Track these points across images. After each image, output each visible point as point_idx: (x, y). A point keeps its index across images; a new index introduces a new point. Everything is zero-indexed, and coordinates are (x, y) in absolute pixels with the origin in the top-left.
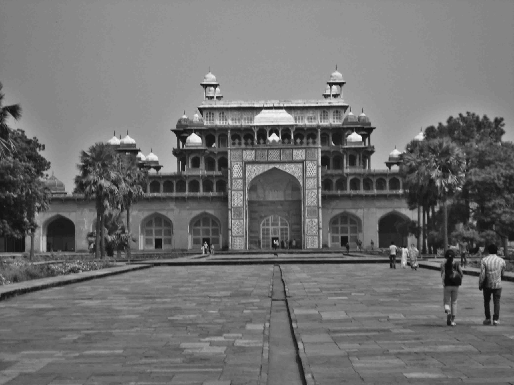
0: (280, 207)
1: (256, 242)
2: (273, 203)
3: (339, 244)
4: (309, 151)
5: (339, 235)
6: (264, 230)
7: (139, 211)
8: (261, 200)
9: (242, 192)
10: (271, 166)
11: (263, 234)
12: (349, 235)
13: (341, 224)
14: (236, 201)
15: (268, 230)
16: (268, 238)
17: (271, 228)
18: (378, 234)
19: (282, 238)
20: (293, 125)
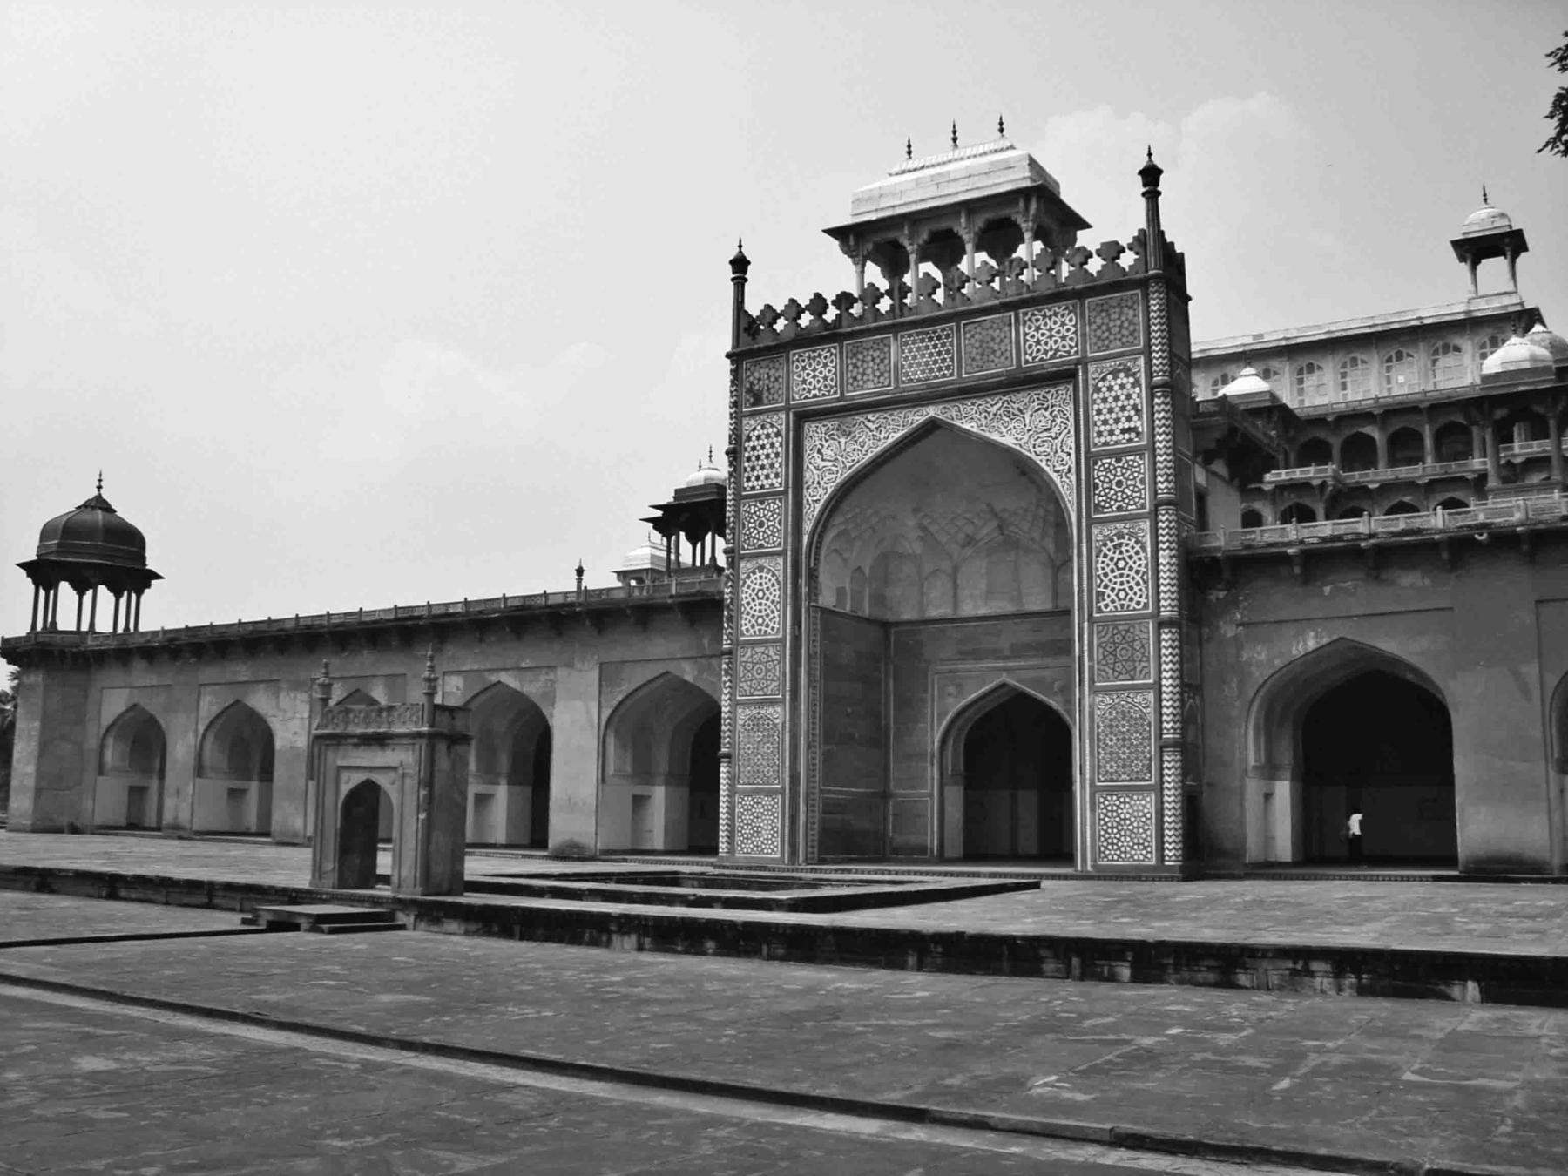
9: (781, 561)
10: (917, 417)
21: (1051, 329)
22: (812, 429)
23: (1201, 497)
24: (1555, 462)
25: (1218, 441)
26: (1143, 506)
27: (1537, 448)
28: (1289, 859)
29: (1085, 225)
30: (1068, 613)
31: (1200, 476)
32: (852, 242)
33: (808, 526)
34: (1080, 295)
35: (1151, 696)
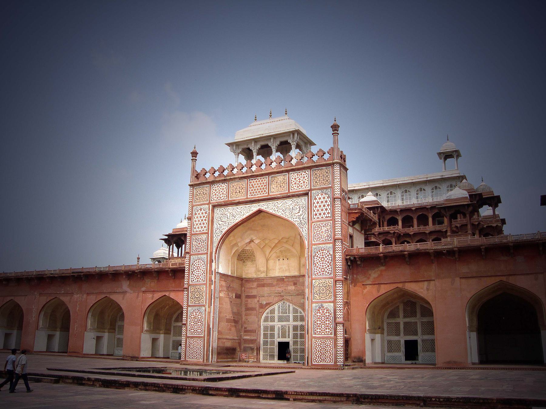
0: (292, 288)
1: (252, 349)
2: (281, 280)
3: (401, 355)
4: (318, 172)
5: (402, 339)
6: (266, 328)
7: (88, 294)
8: (263, 275)
10: (254, 208)
11: (265, 335)
12: (419, 338)
13: (405, 317)
14: (195, 273)
15: (272, 328)
16: (272, 343)
17: (277, 324)
18: (474, 335)
19: (295, 343)
20: (293, 133)
21: (300, 179)
22: (218, 211)
23: (351, 237)
24: (469, 227)
25: (357, 218)
26: (331, 240)
27: (464, 221)
28: (380, 361)
29: (312, 144)
30: (304, 276)
31: (351, 230)
32: (234, 148)
33: (215, 245)
34: (309, 168)
35: (332, 304)
